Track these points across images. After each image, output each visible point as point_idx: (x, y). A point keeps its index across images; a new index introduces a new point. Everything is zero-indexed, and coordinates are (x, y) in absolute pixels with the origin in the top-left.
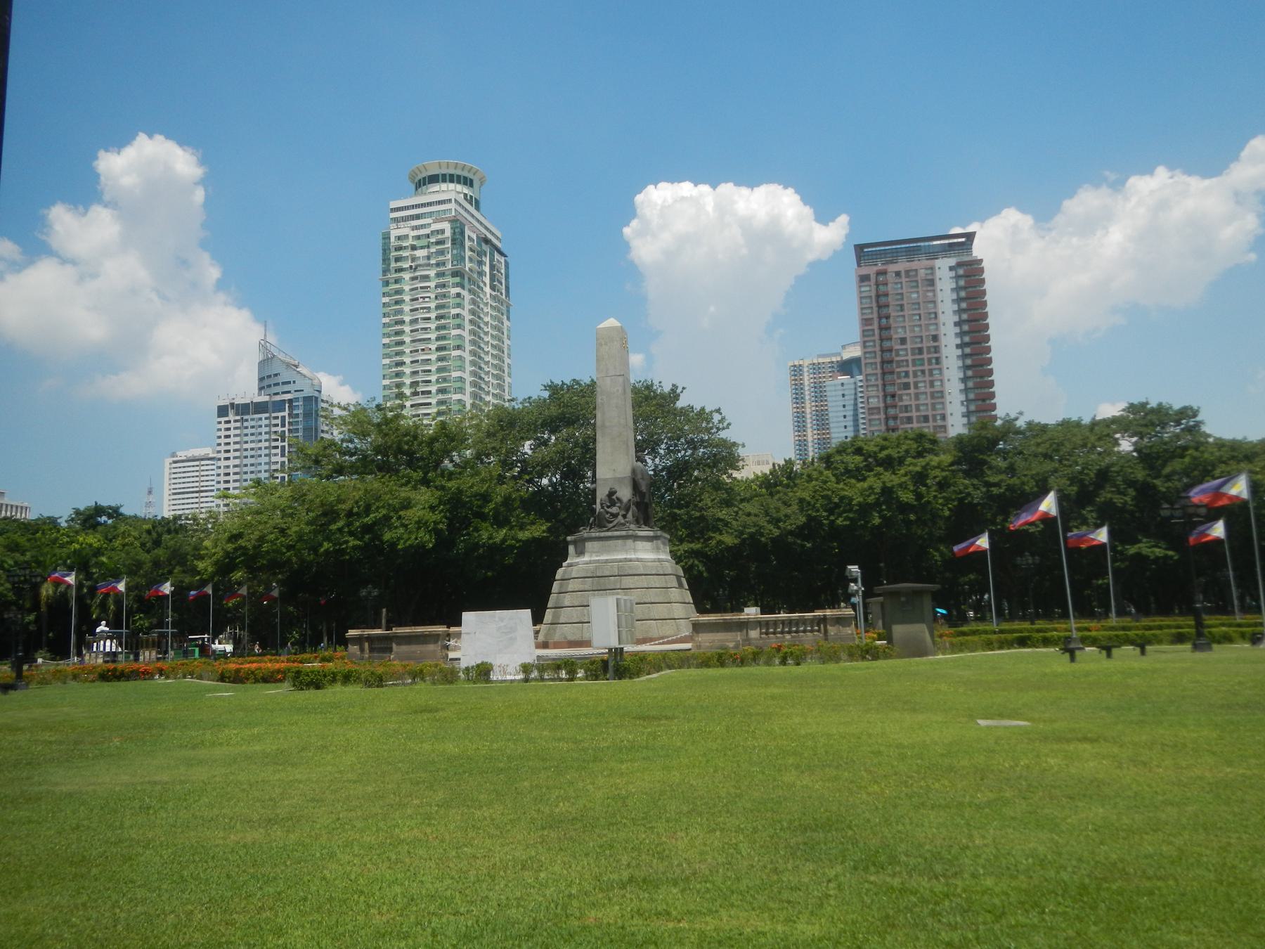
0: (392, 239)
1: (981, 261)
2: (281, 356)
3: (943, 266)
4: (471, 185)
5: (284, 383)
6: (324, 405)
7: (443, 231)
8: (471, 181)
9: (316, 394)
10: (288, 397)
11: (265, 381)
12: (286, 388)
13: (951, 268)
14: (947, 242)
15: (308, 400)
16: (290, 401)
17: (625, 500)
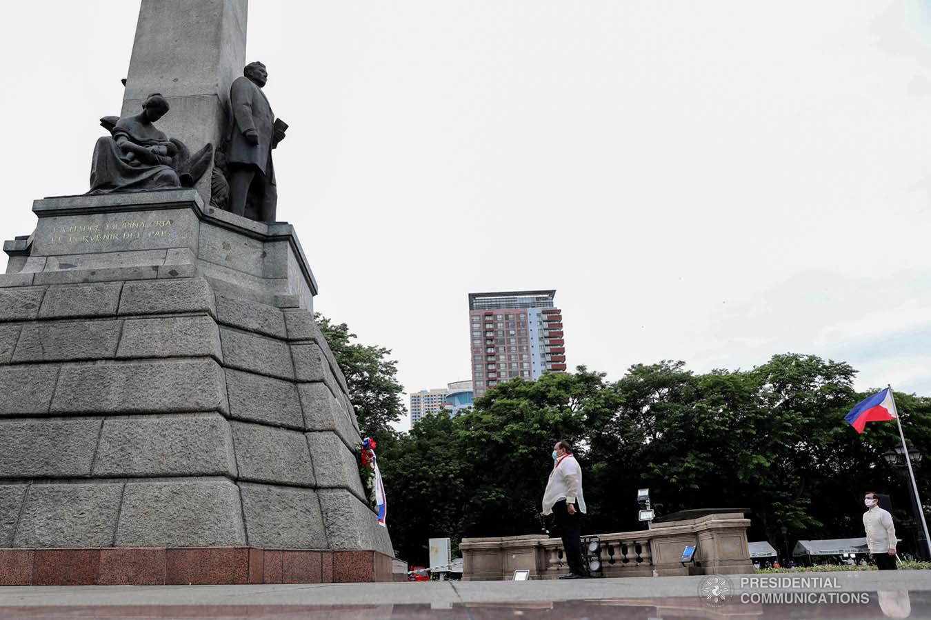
1: (560, 311)
3: (533, 314)
13: (538, 315)
17: (194, 148)
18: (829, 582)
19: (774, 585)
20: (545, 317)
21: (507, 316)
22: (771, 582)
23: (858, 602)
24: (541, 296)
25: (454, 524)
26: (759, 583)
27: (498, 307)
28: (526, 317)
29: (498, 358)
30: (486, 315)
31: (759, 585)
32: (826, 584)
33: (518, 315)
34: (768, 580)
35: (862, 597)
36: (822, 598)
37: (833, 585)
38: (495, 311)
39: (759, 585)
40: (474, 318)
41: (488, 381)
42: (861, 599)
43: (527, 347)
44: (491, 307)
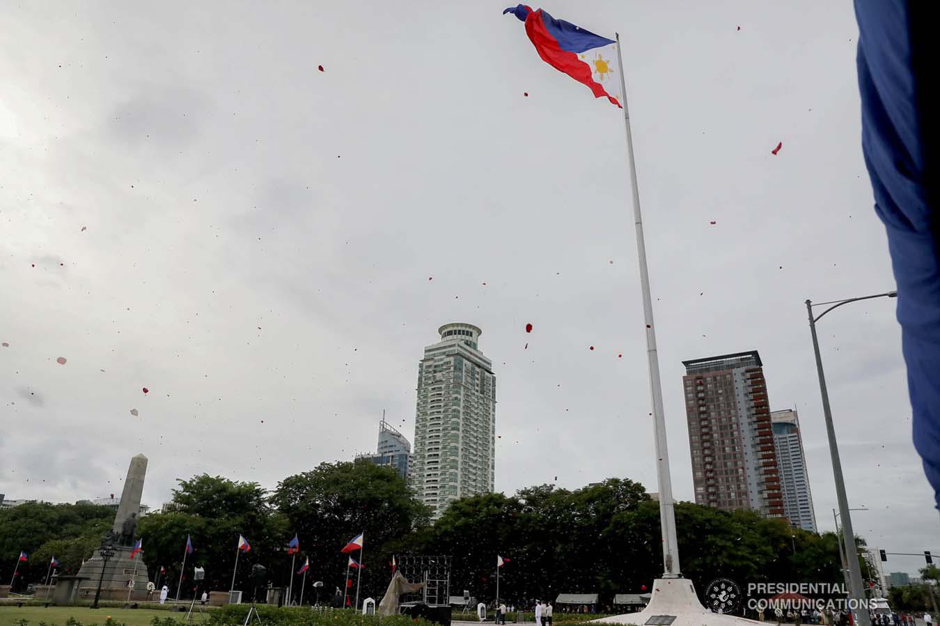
0: (424, 368)
2: (392, 430)
3: (738, 373)
4: (471, 335)
5: (390, 446)
6: (410, 459)
7: (450, 362)
8: (471, 333)
9: (407, 453)
10: (391, 454)
11: (383, 444)
12: (393, 449)
13: (743, 374)
14: (740, 357)
15: (401, 456)
16: (393, 456)
18: (838, 587)
19: (781, 591)
20: (748, 375)
21: (715, 378)
22: (778, 587)
23: (866, 607)
24: (745, 357)
25: (499, 548)
26: (766, 588)
27: (708, 370)
28: (732, 377)
29: (709, 415)
30: (698, 378)
31: (767, 591)
32: (834, 590)
33: (724, 376)
34: (775, 586)
35: (871, 603)
36: (830, 604)
37: (841, 591)
38: (705, 375)
39: (767, 591)
40: (687, 382)
41: (702, 435)
42: (869, 604)
43: (734, 403)
44: (701, 371)
